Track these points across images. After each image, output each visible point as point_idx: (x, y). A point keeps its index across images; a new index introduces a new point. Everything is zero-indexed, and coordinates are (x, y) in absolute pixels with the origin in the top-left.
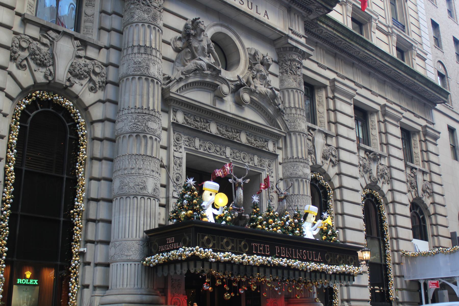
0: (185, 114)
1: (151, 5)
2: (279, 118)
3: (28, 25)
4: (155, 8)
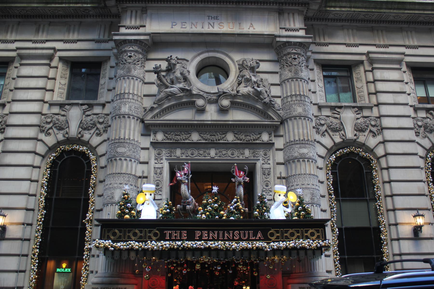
0: (165, 133)
2: (270, 110)
3: (52, 107)
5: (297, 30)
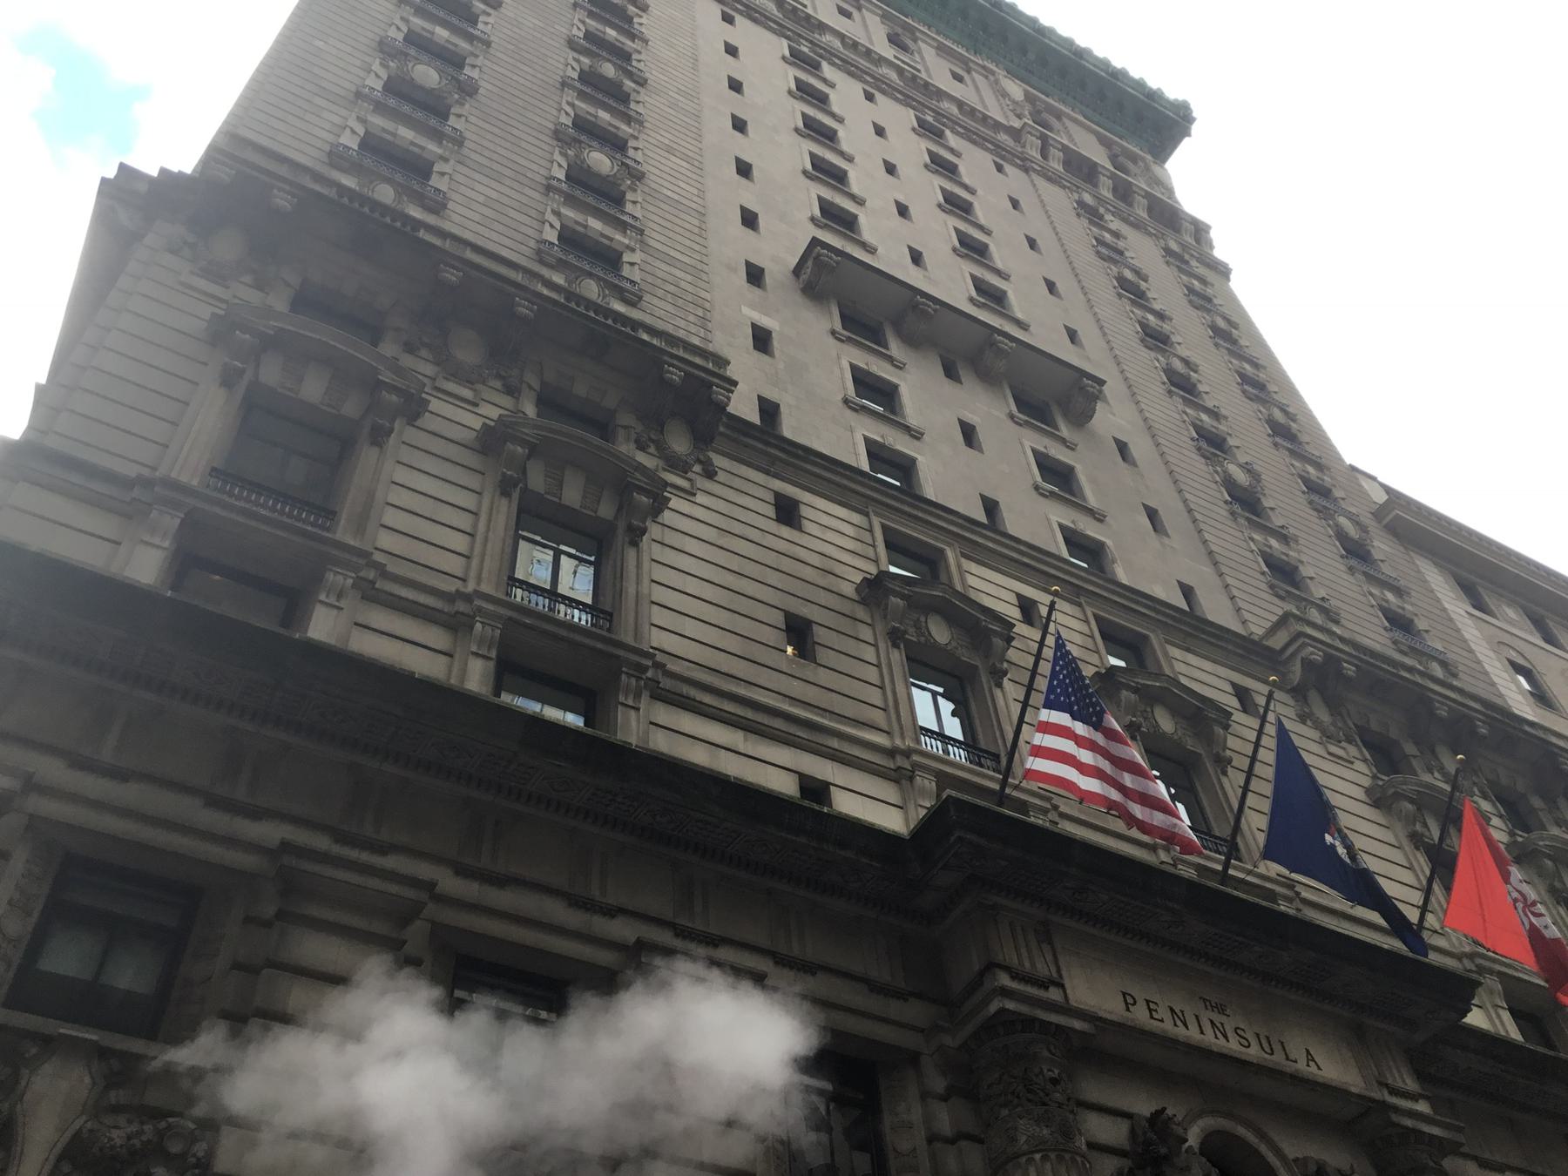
1: (1050, 1100)
4: (1060, 1105)
5: (1414, 1097)
